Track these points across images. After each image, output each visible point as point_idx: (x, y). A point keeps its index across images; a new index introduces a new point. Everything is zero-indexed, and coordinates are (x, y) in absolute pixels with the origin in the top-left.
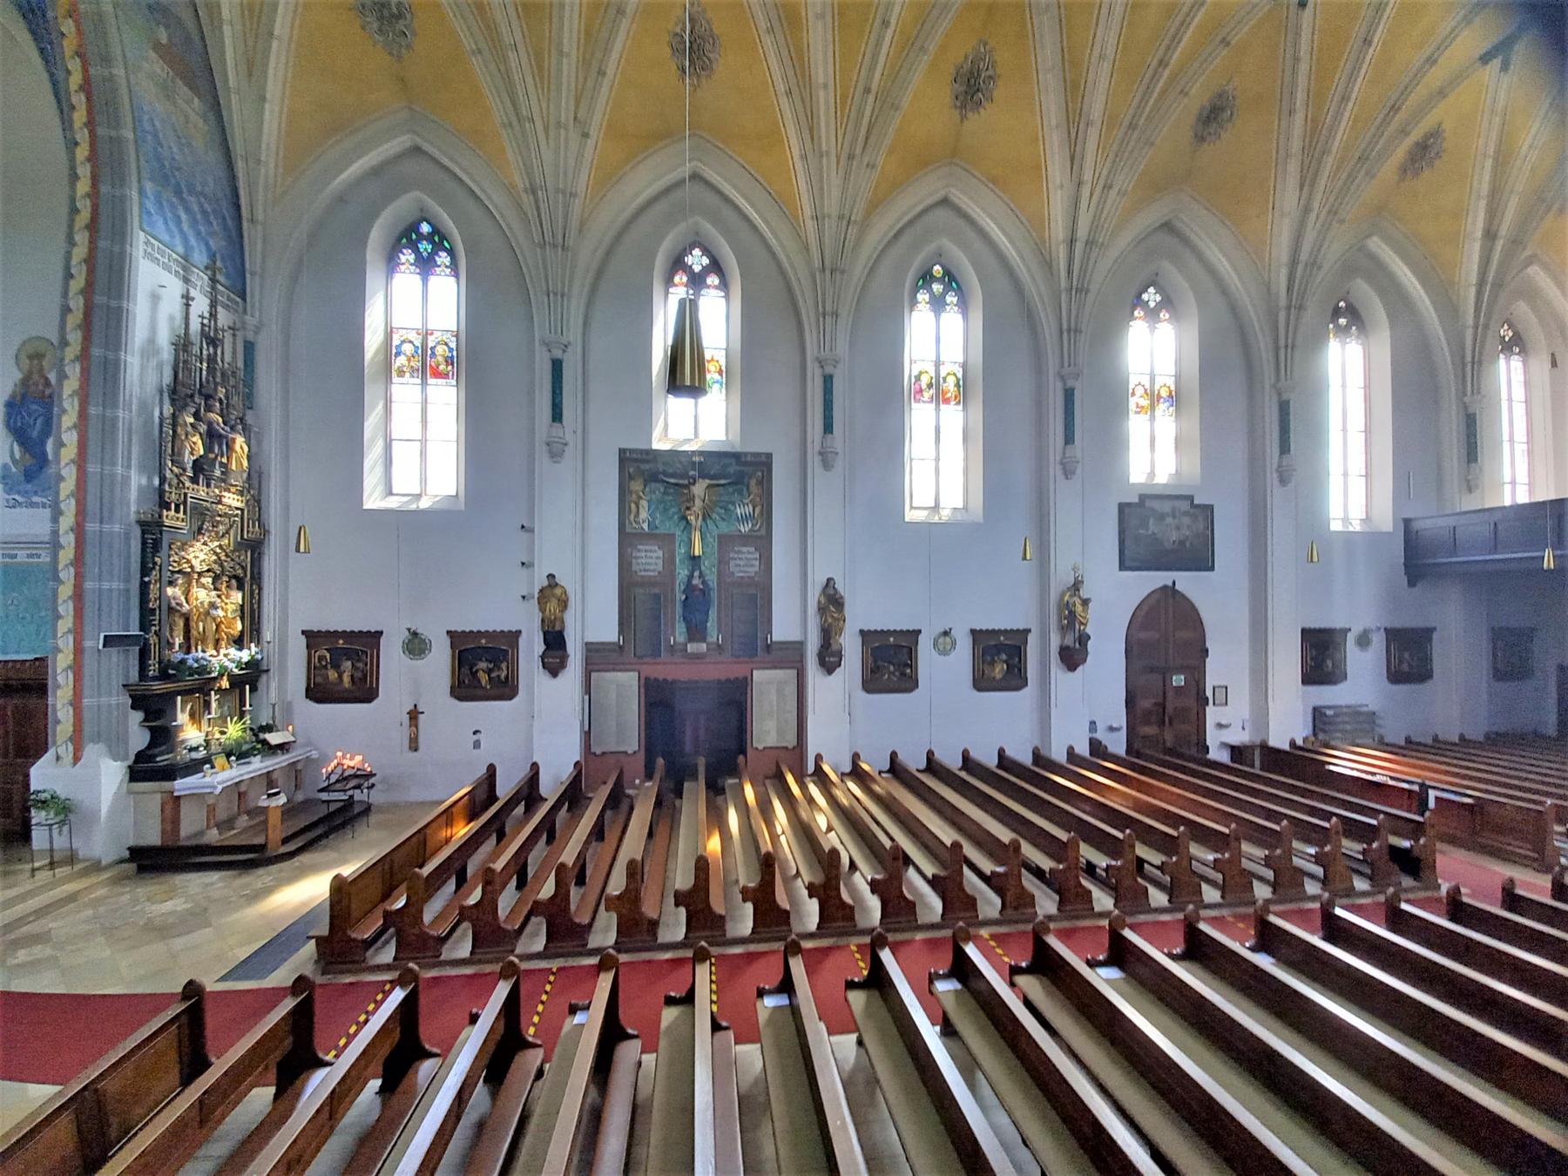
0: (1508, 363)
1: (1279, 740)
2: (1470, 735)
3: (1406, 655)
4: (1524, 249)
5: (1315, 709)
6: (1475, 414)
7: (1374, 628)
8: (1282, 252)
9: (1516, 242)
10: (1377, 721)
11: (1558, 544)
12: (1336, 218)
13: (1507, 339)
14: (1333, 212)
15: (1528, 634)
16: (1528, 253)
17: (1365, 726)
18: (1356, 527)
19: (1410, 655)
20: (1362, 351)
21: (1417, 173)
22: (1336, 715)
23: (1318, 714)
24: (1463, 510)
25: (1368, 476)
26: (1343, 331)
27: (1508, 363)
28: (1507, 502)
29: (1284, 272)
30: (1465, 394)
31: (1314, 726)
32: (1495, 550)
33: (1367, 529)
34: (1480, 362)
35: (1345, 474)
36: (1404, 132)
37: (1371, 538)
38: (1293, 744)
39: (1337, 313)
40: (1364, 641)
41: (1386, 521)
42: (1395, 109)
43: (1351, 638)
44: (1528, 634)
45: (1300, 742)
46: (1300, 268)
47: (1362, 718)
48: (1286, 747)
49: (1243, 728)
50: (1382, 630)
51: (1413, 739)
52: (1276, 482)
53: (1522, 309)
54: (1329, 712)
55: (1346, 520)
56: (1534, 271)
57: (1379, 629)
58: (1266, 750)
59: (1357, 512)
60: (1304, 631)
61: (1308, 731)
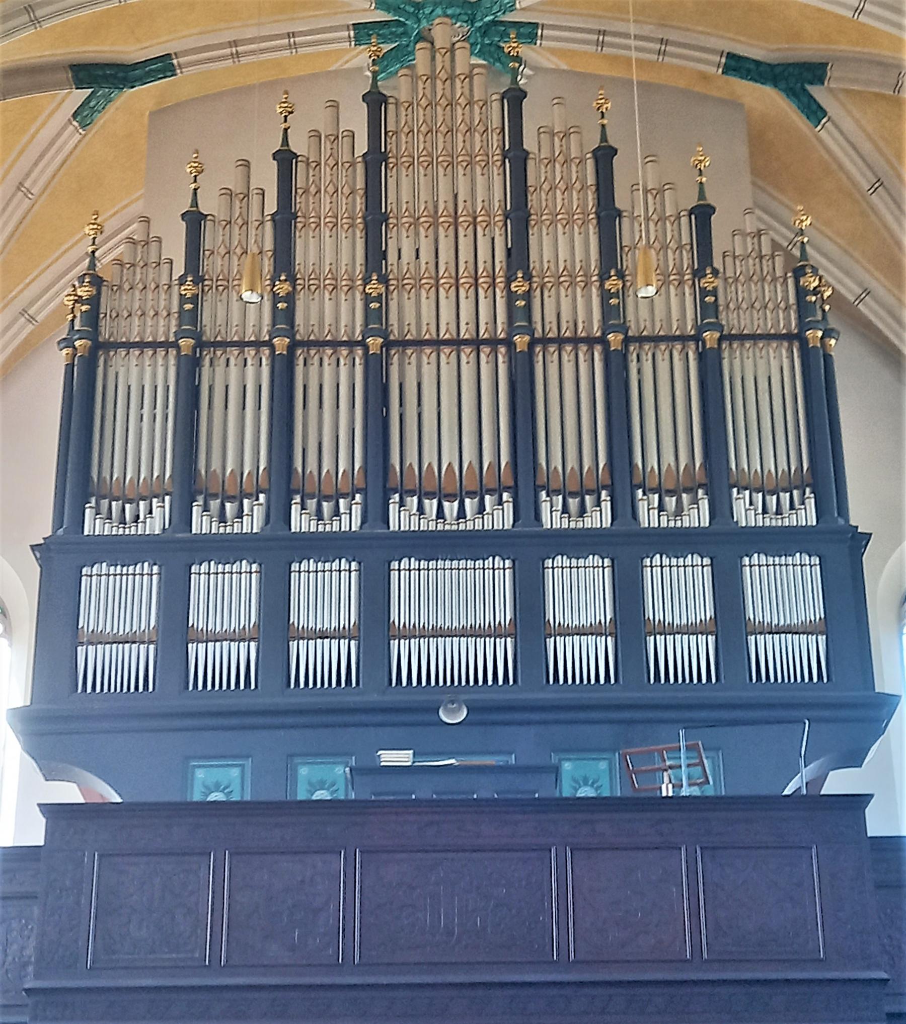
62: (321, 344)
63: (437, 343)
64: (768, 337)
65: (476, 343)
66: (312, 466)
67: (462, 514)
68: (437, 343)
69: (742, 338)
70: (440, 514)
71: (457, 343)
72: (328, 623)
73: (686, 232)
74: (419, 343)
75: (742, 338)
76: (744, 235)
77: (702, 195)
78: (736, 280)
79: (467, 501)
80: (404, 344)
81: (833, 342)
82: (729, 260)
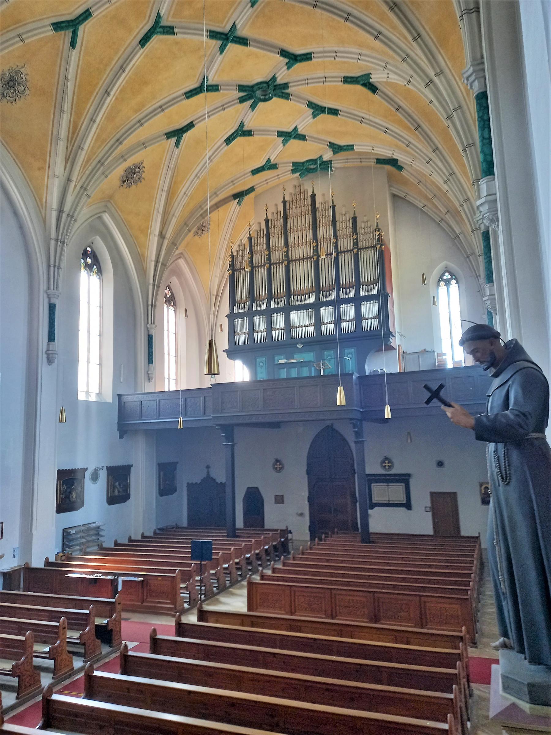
0: (168, 309)
1: (38, 563)
2: (146, 534)
3: (117, 484)
4: (177, 249)
5: (64, 530)
6: (152, 335)
7: (101, 467)
8: (54, 201)
9: (174, 244)
10: (101, 533)
11: (185, 415)
12: (86, 193)
13: (168, 296)
14: (83, 188)
15: (174, 465)
16: (178, 252)
17: (94, 537)
18: (93, 398)
19: (119, 484)
20: (99, 283)
21: (129, 186)
22: (76, 533)
23: (66, 534)
24: (146, 391)
25: (100, 364)
26: (89, 267)
27: (168, 309)
28: (166, 390)
29: (54, 214)
30: (148, 323)
31: (63, 544)
32: (159, 417)
33: (99, 400)
34: (155, 306)
35: (88, 362)
36: (123, 157)
37: (101, 405)
38: (48, 563)
39: (85, 254)
40: (95, 477)
41: (109, 398)
42: (119, 141)
43: (88, 474)
44: (174, 465)
45: (52, 559)
46: (64, 216)
47: (92, 532)
48: (42, 565)
49: (14, 556)
50: (105, 467)
51: (119, 542)
52: (45, 360)
53: (175, 281)
54: (73, 532)
55: (88, 393)
56: (181, 262)
57: (103, 467)
58: (28, 570)
59: (94, 389)
60: (59, 471)
61: (58, 550)
62: (276, 263)
63: (299, 260)
64: (369, 247)
65: (307, 258)
66: (276, 292)
67: (305, 299)
68: (299, 260)
69: (363, 248)
70: (301, 301)
71: (303, 259)
72: (278, 327)
73: (350, 224)
74: (295, 260)
75: (363, 248)
76: (364, 222)
77: (354, 214)
78: (362, 234)
79: (306, 296)
80: (292, 261)
81: (383, 247)
82: (361, 229)
